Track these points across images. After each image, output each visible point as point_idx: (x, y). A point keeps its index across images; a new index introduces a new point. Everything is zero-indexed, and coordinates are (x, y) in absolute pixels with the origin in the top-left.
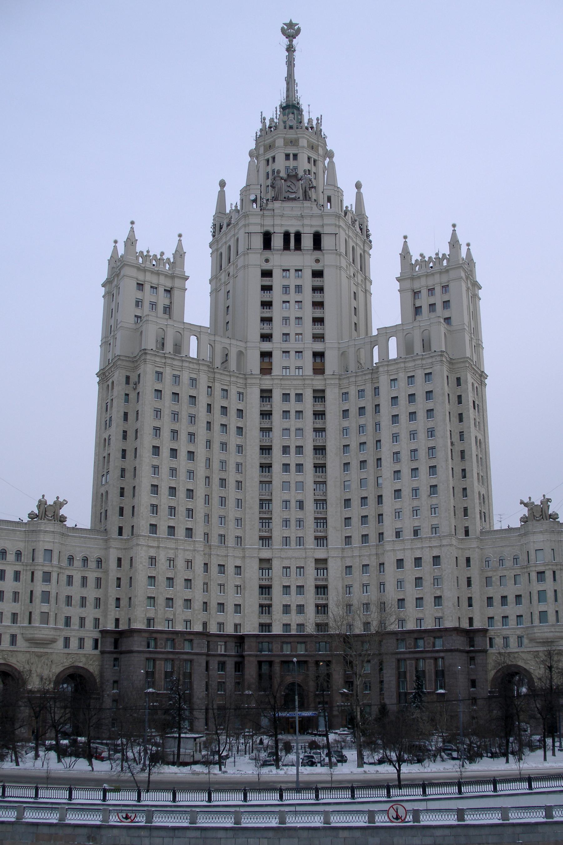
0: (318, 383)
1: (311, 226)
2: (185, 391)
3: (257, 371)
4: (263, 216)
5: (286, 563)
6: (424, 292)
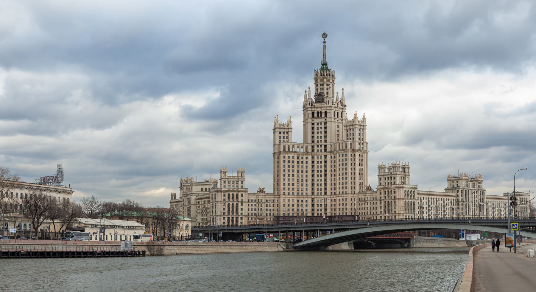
0: (325, 154)
1: (324, 110)
2: (291, 160)
3: (311, 151)
4: (312, 108)
5: (318, 199)
6: (349, 130)
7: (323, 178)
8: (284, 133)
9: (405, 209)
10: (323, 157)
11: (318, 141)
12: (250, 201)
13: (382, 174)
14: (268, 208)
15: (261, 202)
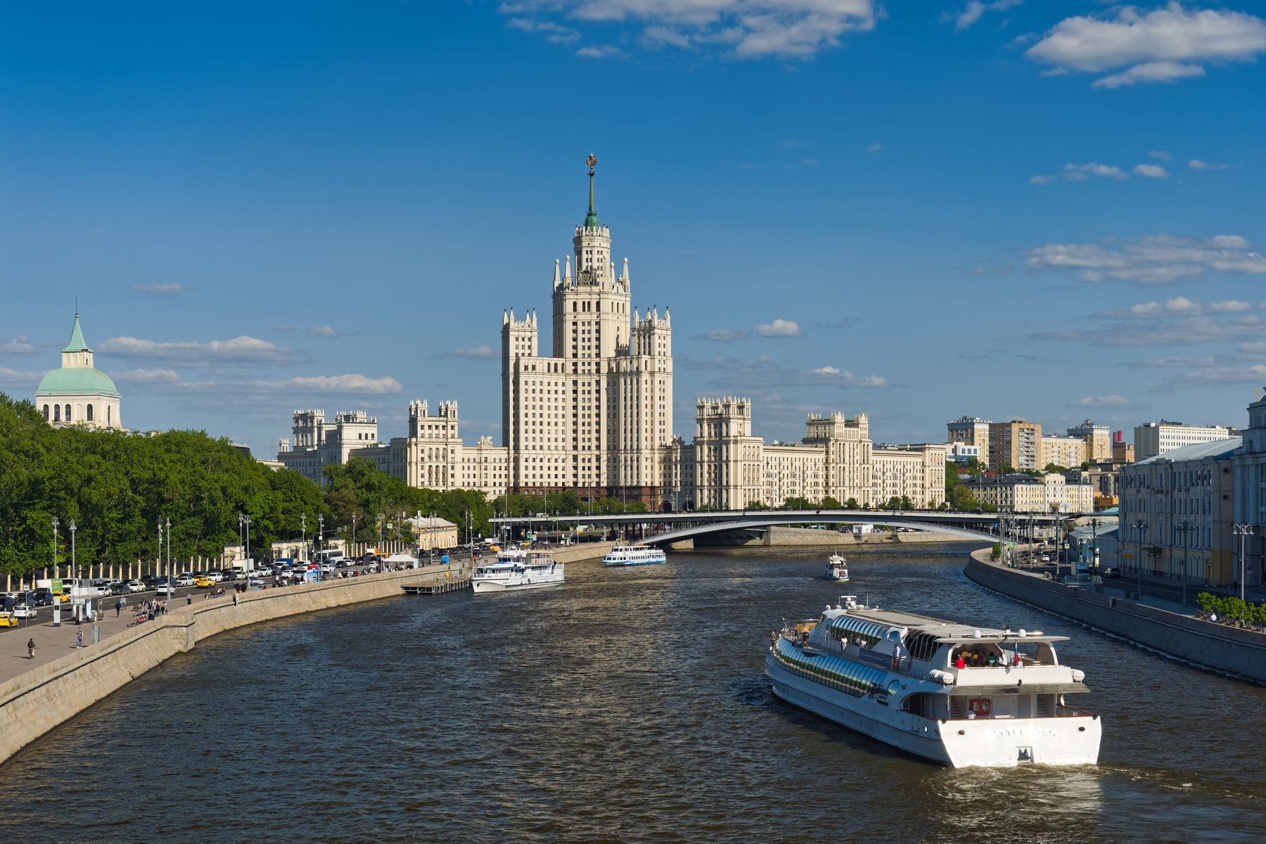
2: (538, 388)
3: (571, 372)
7: (594, 419)
8: (523, 339)
9: (744, 478)
10: (594, 383)
11: (583, 354)
12: (466, 460)
13: (705, 417)
14: (497, 472)
15: (486, 461)
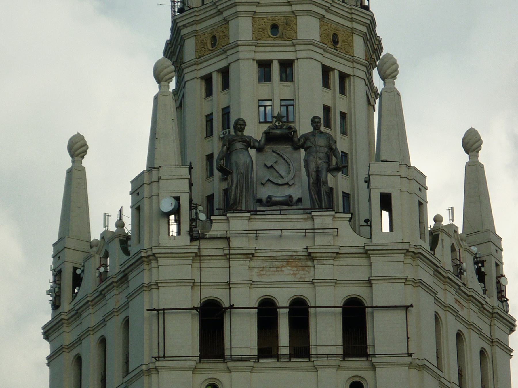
1: (336, 283)
4: (198, 256)
